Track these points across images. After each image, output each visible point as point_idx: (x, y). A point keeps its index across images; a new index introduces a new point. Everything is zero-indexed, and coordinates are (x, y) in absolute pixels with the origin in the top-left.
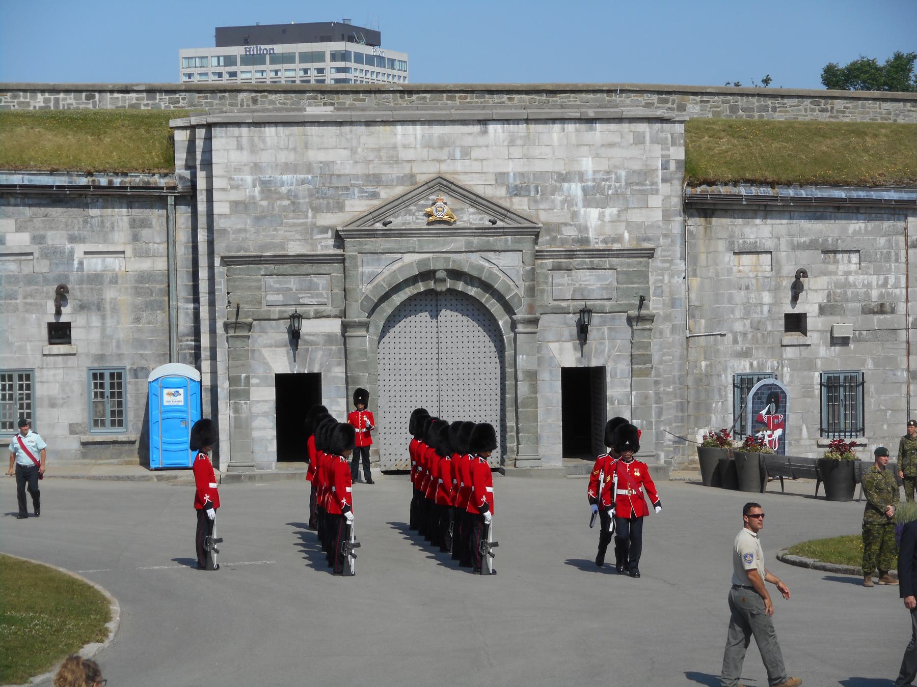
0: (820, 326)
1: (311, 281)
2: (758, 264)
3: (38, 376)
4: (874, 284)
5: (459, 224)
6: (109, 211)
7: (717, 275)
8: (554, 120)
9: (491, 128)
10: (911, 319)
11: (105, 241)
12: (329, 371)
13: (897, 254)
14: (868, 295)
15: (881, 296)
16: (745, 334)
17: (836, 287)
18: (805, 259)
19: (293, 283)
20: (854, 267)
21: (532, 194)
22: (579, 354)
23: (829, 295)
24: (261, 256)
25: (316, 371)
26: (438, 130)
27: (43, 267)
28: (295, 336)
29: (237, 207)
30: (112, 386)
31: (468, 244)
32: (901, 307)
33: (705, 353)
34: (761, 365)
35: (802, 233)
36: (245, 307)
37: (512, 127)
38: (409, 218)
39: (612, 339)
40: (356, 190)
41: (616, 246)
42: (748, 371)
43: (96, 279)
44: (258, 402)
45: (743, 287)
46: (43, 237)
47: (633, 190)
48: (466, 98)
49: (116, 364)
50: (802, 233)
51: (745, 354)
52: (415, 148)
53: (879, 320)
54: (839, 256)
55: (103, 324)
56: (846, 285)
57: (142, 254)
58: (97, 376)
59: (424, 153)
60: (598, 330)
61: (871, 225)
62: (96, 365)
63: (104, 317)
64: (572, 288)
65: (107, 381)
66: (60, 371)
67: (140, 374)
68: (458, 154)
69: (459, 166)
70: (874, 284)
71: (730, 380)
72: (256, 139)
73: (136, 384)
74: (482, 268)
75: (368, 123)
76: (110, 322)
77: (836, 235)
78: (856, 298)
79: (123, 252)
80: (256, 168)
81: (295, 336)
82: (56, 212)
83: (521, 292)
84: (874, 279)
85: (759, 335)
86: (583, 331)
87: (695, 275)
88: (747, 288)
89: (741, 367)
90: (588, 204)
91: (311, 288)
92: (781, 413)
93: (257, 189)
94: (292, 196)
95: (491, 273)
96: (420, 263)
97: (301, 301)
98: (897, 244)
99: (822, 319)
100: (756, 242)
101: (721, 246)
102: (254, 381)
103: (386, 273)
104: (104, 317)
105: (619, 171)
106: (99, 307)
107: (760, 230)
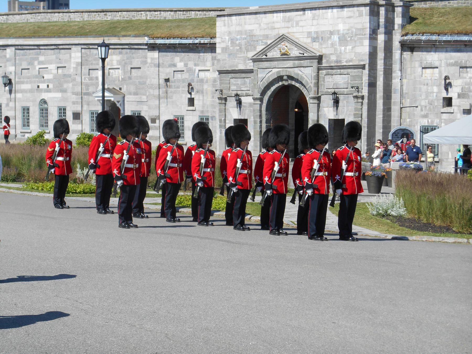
0: (458, 104)
1: (245, 81)
2: (433, 73)
3: (185, 118)
5: (292, 55)
8: (328, 7)
9: (306, 12)
11: (205, 66)
16: (426, 107)
19: (239, 81)
21: (320, 41)
22: (335, 113)
24: (228, 70)
26: (288, 14)
27: (185, 76)
28: (239, 103)
29: (225, 50)
31: (294, 64)
33: (409, 114)
34: (432, 122)
36: (224, 91)
37: (314, 12)
38: (275, 53)
41: (351, 64)
42: (426, 124)
43: (202, 81)
45: (426, 84)
46: (187, 64)
47: (358, 38)
49: (207, 114)
51: (425, 116)
52: (280, 22)
55: (203, 98)
57: (214, 71)
59: (283, 25)
63: (203, 96)
64: (333, 83)
66: (191, 117)
69: (295, 30)
71: (419, 129)
73: (212, 122)
74: (298, 74)
75: (265, 13)
76: (205, 98)
79: (209, 70)
80: (230, 33)
81: (239, 103)
82: (191, 55)
83: (312, 85)
85: (432, 107)
86: (336, 102)
87: (406, 78)
88: (427, 85)
89: (424, 122)
90: (340, 45)
91: (245, 83)
93: (230, 42)
94: (240, 45)
95: (301, 77)
96: (278, 72)
97: (242, 89)
99: (459, 100)
100: (431, 63)
101: (417, 64)
102: (227, 121)
103: (267, 76)
104: (203, 96)
105: (352, 29)
106: (202, 92)
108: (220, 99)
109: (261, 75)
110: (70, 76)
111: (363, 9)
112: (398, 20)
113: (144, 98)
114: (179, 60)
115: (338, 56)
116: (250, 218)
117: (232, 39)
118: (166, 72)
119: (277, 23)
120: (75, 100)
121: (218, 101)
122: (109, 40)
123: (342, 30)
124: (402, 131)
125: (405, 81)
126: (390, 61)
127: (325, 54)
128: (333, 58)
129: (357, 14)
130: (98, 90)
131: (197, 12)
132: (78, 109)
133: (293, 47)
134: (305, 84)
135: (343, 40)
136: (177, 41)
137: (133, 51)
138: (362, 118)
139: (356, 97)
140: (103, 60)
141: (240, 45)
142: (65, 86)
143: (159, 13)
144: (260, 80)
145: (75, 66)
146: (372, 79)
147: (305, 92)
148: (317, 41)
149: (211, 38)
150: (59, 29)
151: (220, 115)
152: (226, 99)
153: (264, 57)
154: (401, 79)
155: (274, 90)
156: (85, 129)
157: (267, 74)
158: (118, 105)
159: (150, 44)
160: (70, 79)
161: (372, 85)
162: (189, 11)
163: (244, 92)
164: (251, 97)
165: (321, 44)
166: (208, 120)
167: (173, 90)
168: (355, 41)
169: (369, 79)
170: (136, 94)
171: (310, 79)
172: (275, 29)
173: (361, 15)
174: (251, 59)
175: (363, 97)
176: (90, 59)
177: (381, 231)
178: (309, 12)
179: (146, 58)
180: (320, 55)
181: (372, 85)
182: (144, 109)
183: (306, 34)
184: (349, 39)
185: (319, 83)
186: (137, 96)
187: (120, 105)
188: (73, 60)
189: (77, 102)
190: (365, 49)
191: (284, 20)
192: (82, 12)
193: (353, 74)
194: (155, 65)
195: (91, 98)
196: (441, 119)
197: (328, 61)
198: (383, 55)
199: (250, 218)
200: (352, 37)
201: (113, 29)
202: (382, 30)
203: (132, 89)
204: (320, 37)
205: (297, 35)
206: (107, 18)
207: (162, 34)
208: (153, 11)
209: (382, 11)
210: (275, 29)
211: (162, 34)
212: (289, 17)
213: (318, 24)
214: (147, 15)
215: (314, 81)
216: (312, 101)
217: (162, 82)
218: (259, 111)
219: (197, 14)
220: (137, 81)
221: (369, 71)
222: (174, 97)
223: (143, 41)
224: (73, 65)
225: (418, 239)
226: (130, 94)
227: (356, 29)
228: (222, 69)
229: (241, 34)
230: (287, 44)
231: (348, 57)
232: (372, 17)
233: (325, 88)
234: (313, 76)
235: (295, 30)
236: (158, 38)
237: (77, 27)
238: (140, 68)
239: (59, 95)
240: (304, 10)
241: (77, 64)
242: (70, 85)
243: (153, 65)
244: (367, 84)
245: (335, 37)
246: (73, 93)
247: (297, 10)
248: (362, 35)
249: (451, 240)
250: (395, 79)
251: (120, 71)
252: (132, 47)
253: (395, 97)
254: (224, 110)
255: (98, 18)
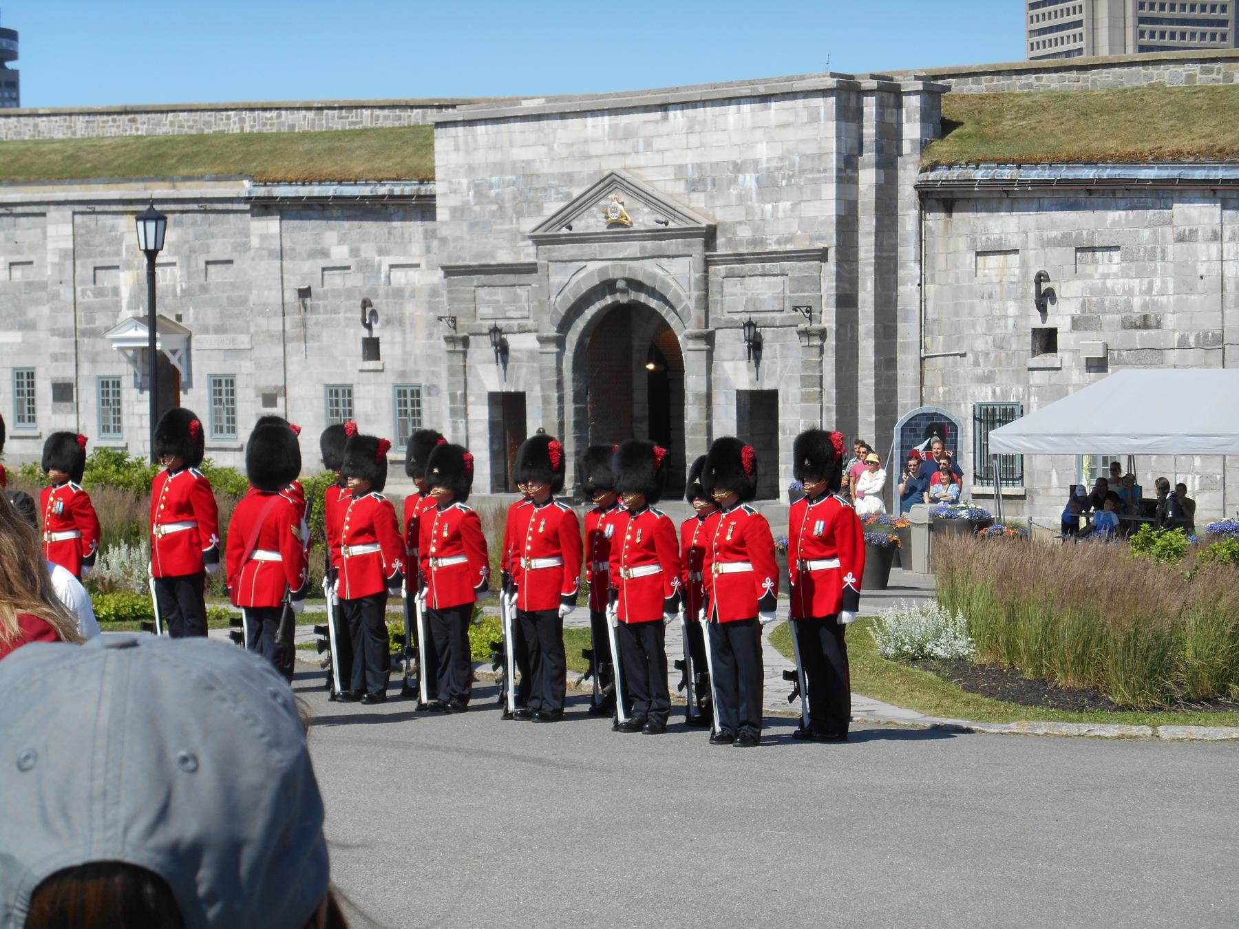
0: (1072, 345)
1: (515, 293)
4: (1137, 289)
5: (636, 227)
6: (408, 223)
7: (957, 281)
9: (671, 113)
10: (1177, 336)
11: (405, 253)
12: (532, 390)
13: (1163, 251)
14: (1129, 305)
15: (1145, 305)
16: (987, 354)
17: (1091, 294)
18: (1057, 261)
19: (500, 294)
20: (1115, 268)
21: (709, 187)
22: (753, 375)
23: (1083, 305)
25: (521, 390)
27: (354, 280)
28: (502, 350)
29: (458, 212)
30: (413, 405)
31: (643, 249)
32: (1169, 320)
34: (1005, 393)
35: (1053, 225)
36: (461, 321)
37: (690, 112)
38: (592, 221)
39: (784, 357)
40: (553, 191)
41: (790, 247)
42: (990, 400)
43: (398, 293)
44: (475, 421)
45: (986, 295)
48: (992, 80)
49: (414, 381)
50: (1053, 225)
51: (987, 379)
53: (1142, 337)
54: (1098, 254)
55: (404, 339)
56: (1104, 291)
57: (431, 267)
58: (401, 393)
59: (611, 147)
60: (771, 347)
61: (1132, 214)
62: (399, 382)
63: (404, 332)
64: (744, 298)
65: (409, 398)
67: (433, 392)
68: (641, 148)
69: (641, 160)
70: (1137, 289)
72: (470, 138)
75: (563, 116)
77: (1092, 227)
78: (1114, 309)
79: (417, 266)
80: (471, 169)
81: (502, 350)
82: (370, 226)
83: (692, 304)
84: (1136, 283)
85: (1003, 355)
86: (755, 347)
87: (933, 282)
88: (990, 297)
89: (983, 395)
90: (762, 200)
91: (515, 300)
92: (950, 448)
93: (471, 193)
94: (499, 200)
95: (663, 282)
96: (603, 271)
97: (509, 314)
98: (1164, 237)
99: (1075, 334)
100: (1001, 239)
101: (963, 243)
102: (470, 399)
103: (573, 282)
104: (404, 332)
106: (401, 323)
107: (1004, 225)
108: (450, 340)
109: (557, 279)
110: (43, 286)
111: (818, 102)
112: (912, 130)
113: (243, 341)
114: (337, 240)
115: (756, 229)
116: (579, 682)
117: (477, 186)
118: (302, 271)
119: (595, 143)
120: (57, 350)
121: (444, 346)
122: (146, 189)
123: (765, 158)
124: (927, 419)
125: (930, 289)
126: (890, 238)
127: (723, 223)
128: (744, 233)
129: (804, 116)
130: (119, 321)
131: (377, 112)
132: (66, 372)
133: (639, 205)
134: (673, 302)
135: (769, 186)
136: (330, 190)
137: (212, 216)
138: (821, 386)
139: (806, 333)
140: (151, 255)
141: (499, 200)
142: (32, 313)
143: (274, 113)
144: (554, 291)
145: (57, 260)
146: (847, 286)
147: (673, 321)
148: (701, 188)
149: (421, 182)
150: (12, 161)
151: (450, 384)
152: (465, 342)
153: (565, 231)
154: (920, 285)
155: (594, 317)
156: (84, 427)
157: (572, 275)
158: (174, 360)
159: (257, 198)
160: (43, 294)
161: (846, 301)
162: (357, 107)
163: (515, 323)
164: (533, 336)
165: (712, 197)
166: (418, 395)
167: (321, 317)
168: (800, 189)
169: (837, 287)
170: (220, 330)
171: (686, 288)
172: (590, 157)
173: (814, 119)
174: (531, 237)
175: (822, 334)
176: (97, 241)
177: (923, 707)
178: (679, 112)
179: (247, 235)
180: (709, 227)
181: (846, 301)
182: (244, 370)
183: (671, 171)
184: (784, 182)
185: (711, 298)
186: (224, 336)
187: (179, 360)
188: (50, 245)
189: (65, 354)
190: (826, 207)
191: (614, 135)
192: (70, 114)
193: (797, 274)
194: (271, 254)
195: (100, 345)
196: (1028, 386)
197: (729, 242)
198: (874, 222)
199: (579, 682)
200: (790, 177)
201: (154, 159)
202: (869, 156)
203: (211, 316)
204: (709, 180)
205: (649, 175)
206: (137, 129)
207: (288, 172)
208: (258, 109)
209: (870, 106)
210: (590, 157)
211: (288, 172)
212: (625, 127)
213: (702, 145)
214: (242, 120)
215: (695, 294)
216: (691, 345)
217: (291, 297)
218: (554, 372)
219: (378, 117)
220: (225, 295)
221: (838, 265)
222: (325, 338)
223: (237, 190)
224: (52, 258)
225: (1025, 730)
226: (205, 330)
227: (803, 156)
228: (453, 264)
229: (502, 172)
230: (623, 198)
231: (782, 229)
232: (843, 124)
233: (725, 311)
234: (692, 280)
235: (641, 160)
236: (278, 182)
237: (59, 157)
238: (231, 262)
239: (15, 337)
240: (664, 107)
241: (63, 254)
242: (45, 310)
243: (265, 253)
244: (833, 300)
245: (748, 176)
246: (54, 332)
247: (647, 109)
248: (819, 171)
249: (1111, 730)
250: (904, 284)
251: (177, 271)
252: (209, 206)
253: (907, 332)
254: (461, 369)
255: (114, 129)
